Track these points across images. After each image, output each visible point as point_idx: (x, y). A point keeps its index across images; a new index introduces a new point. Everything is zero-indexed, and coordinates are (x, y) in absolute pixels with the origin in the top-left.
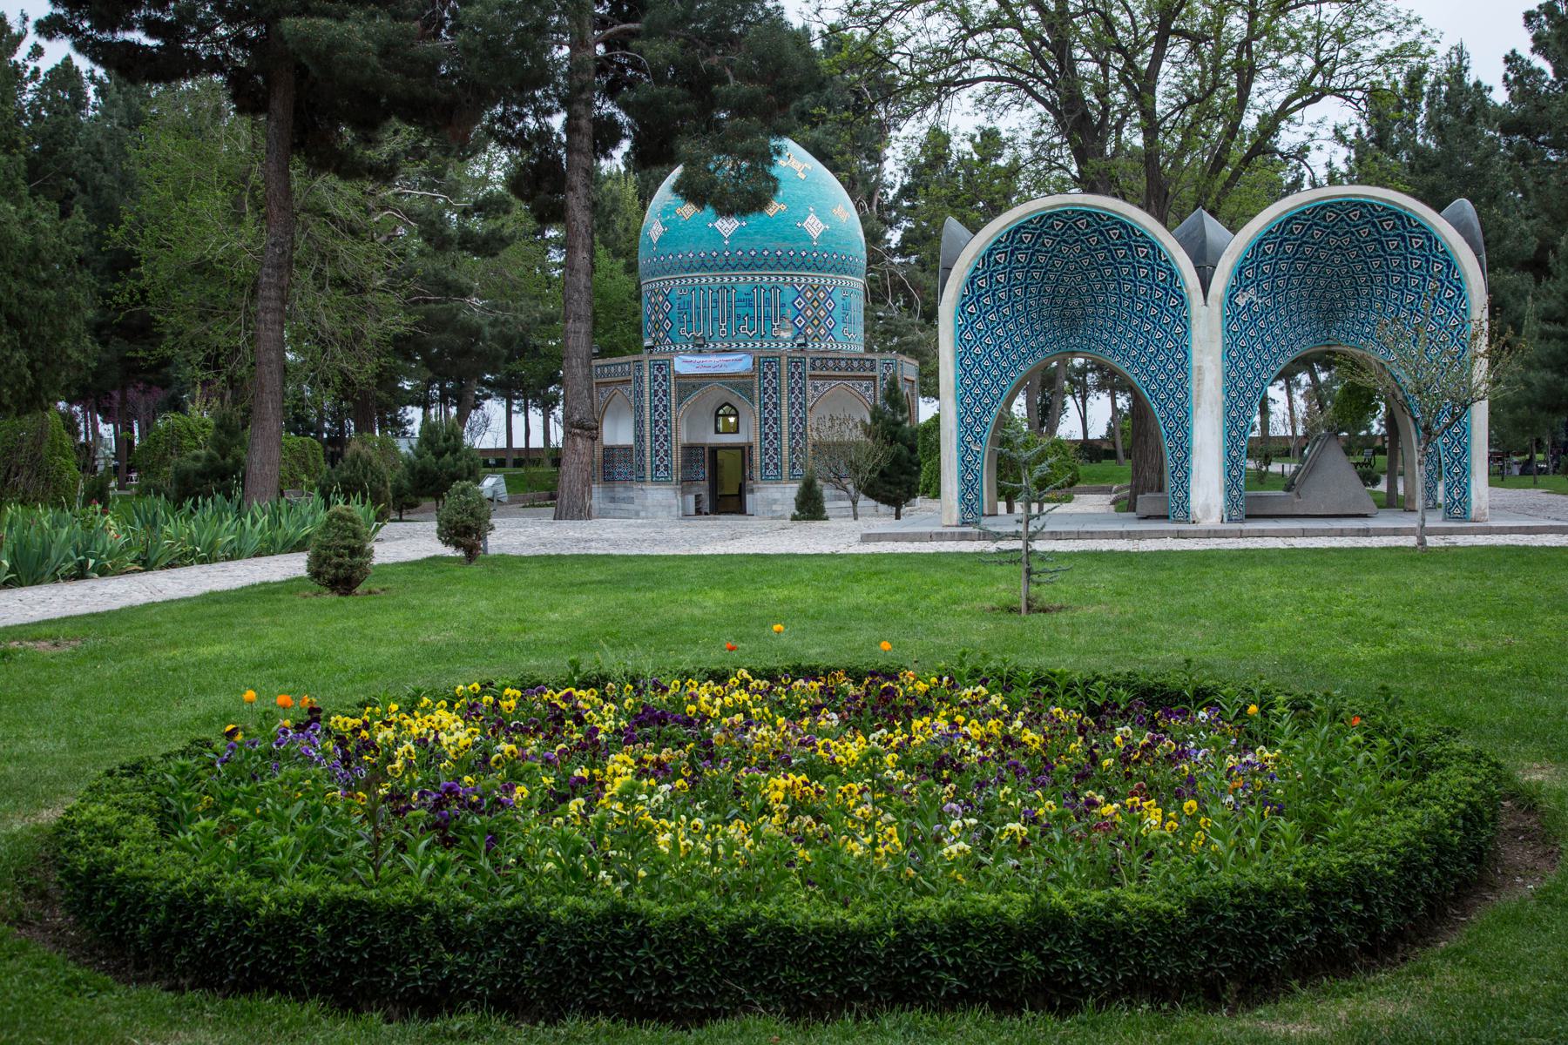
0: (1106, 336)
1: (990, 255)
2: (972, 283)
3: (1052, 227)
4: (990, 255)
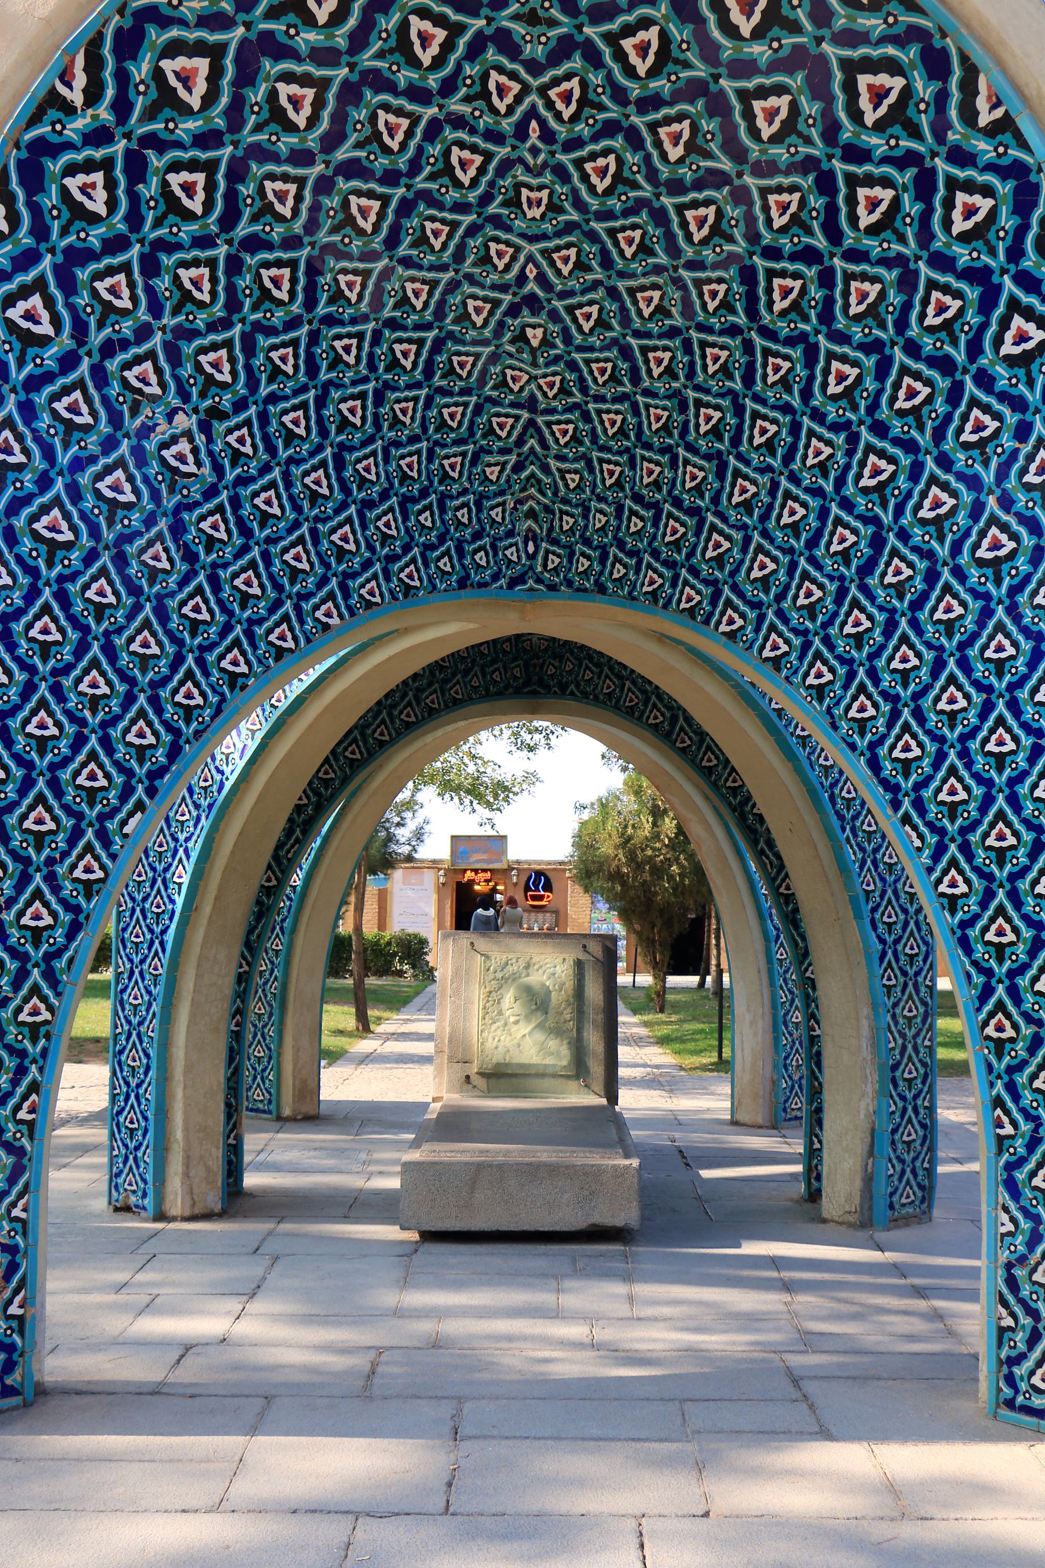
0: (675, 528)
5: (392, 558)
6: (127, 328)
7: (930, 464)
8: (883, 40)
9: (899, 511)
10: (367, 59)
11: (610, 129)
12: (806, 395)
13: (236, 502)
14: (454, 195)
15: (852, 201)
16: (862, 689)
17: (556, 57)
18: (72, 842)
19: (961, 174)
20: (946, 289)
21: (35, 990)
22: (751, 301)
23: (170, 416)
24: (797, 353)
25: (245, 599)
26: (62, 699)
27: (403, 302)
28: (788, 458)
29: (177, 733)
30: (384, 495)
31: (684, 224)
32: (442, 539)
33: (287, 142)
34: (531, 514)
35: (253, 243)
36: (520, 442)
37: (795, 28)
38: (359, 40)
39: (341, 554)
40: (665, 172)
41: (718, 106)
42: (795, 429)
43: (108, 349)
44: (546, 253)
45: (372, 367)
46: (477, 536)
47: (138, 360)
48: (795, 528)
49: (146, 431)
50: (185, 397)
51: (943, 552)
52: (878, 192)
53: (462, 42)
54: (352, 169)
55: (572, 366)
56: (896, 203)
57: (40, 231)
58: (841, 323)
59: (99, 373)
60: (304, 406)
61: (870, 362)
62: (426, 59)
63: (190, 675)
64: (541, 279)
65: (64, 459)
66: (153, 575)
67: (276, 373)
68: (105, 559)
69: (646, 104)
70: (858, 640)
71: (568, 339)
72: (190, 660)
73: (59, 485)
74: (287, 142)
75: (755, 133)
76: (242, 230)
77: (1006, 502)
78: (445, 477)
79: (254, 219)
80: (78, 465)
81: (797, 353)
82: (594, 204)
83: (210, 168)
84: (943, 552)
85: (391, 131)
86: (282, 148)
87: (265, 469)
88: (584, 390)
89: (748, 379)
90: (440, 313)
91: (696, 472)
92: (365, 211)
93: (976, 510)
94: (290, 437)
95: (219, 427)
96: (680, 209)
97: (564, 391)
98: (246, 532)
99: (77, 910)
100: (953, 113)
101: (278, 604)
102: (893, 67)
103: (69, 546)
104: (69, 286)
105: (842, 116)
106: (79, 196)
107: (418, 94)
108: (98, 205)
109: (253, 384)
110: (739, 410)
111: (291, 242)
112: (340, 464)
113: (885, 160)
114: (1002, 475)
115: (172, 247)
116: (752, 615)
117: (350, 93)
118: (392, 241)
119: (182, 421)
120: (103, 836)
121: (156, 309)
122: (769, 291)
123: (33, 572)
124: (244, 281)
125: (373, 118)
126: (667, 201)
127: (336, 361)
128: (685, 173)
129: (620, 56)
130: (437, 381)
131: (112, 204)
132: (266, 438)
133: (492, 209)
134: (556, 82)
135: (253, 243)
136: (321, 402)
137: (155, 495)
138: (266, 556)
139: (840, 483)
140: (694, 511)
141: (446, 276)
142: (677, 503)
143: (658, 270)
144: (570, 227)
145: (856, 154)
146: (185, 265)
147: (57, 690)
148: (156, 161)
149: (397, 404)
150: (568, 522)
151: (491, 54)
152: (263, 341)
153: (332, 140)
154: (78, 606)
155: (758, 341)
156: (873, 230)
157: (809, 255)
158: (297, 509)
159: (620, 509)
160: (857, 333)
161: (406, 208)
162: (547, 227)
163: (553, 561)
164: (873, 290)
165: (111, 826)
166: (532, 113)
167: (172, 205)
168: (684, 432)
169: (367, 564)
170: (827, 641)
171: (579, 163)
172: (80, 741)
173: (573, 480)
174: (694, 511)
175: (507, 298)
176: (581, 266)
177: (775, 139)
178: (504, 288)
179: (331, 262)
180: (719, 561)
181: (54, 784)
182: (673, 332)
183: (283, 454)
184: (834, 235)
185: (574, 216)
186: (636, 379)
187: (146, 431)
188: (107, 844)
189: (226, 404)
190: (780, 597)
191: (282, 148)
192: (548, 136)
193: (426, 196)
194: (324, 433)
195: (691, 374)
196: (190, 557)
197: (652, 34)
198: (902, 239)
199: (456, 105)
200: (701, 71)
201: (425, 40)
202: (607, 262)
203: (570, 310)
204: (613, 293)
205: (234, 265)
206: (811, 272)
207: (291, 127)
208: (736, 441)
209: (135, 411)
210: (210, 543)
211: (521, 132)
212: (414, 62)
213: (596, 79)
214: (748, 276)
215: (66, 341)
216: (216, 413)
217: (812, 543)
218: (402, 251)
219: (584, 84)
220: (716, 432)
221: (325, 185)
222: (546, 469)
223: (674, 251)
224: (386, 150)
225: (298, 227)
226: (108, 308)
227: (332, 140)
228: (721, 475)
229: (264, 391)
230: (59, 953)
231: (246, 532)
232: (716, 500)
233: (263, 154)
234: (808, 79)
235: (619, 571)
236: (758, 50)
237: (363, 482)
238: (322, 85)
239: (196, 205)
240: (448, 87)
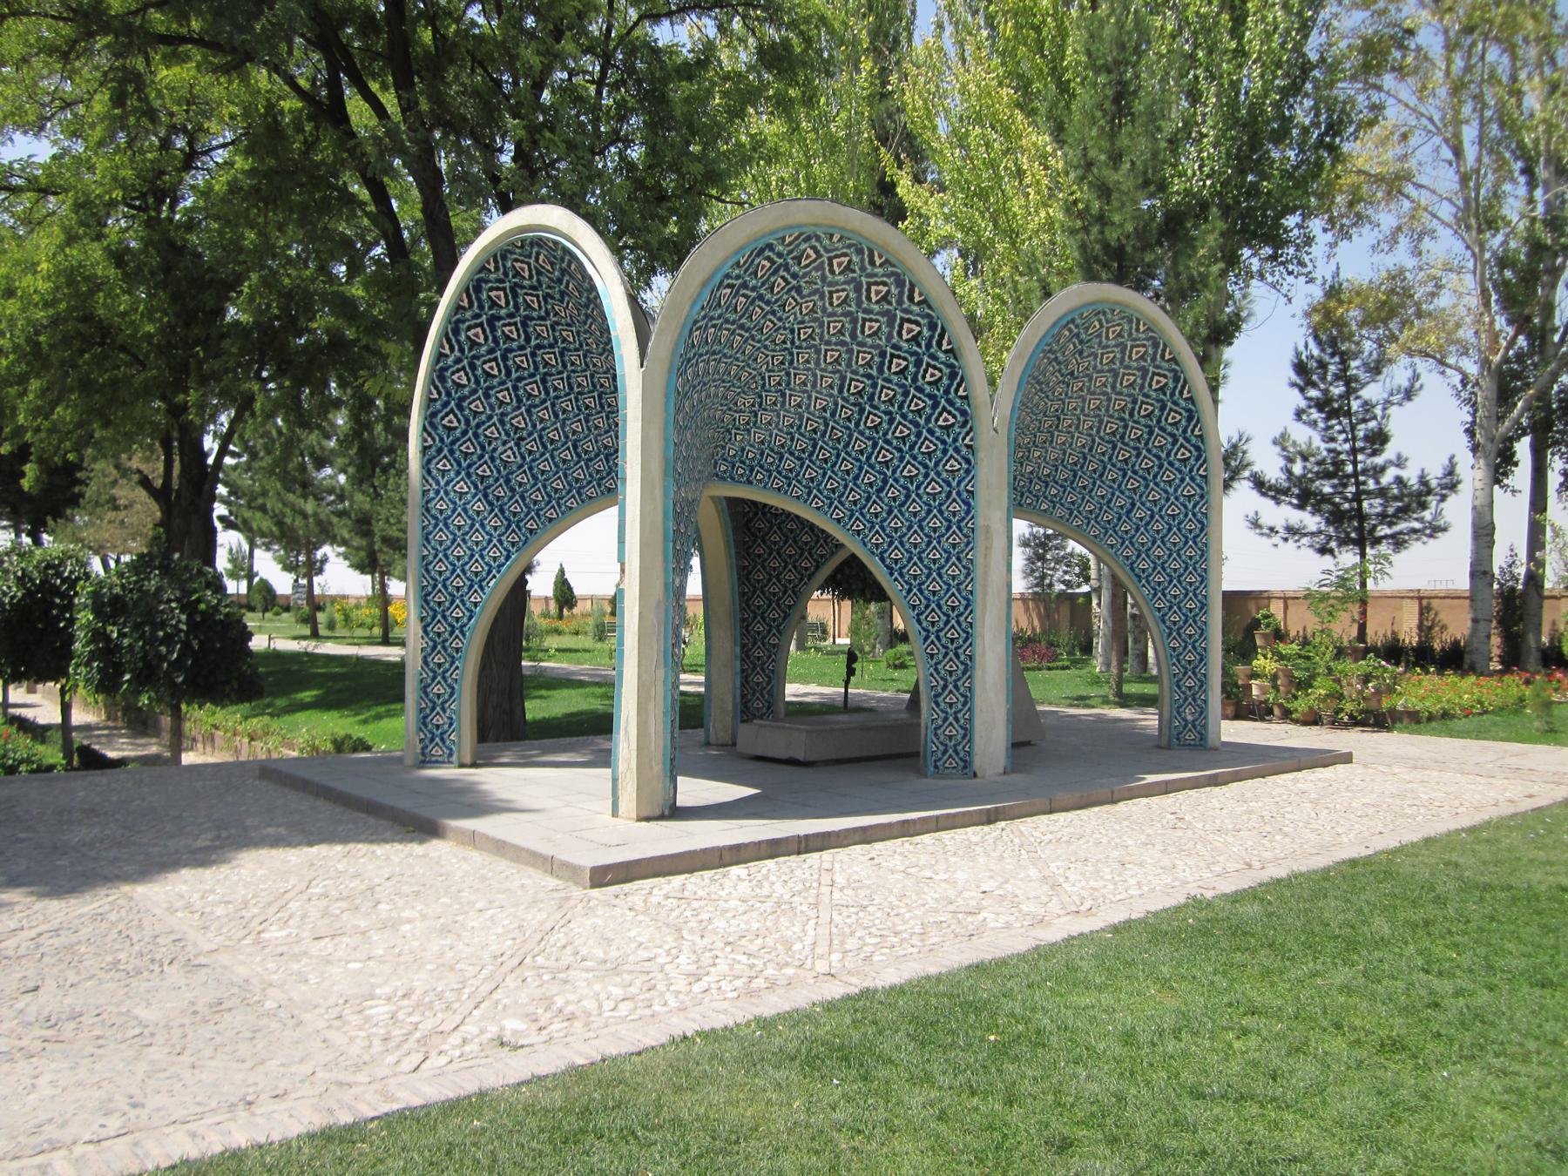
1: (456, 332)
2: (442, 379)
6: (483, 417)
13: (531, 469)
27: (579, 385)
30: (597, 455)
33: (515, 345)
35: (519, 379)
43: (478, 426)
49: (494, 450)
50: (508, 434)
54: (539, 347)
57: (448, 394)
65: (464, 465)
66: (498, 498)
67: (542, 420)
76: (514, 376)
80: (469, 466)
83: (495, 359)
104: (461, 409)
108: (465, 382)
109: (534, 426)
112: (575, 447)
115: (492, 388)
118: (564, 366)
121: (492, 409)
124: (521, 392)
127: (564, 411)
135: (519, 379)
136: (563, 426)
148: (478, 363)
153: (528, 339)
167: (488, 375)
187: (494, 450)
189: (525, 434)
196: (513, 490)
205: (515, 388)
210: (521, 484)
215: (463, 426)
237: (586, 452)
239: (496, 372)
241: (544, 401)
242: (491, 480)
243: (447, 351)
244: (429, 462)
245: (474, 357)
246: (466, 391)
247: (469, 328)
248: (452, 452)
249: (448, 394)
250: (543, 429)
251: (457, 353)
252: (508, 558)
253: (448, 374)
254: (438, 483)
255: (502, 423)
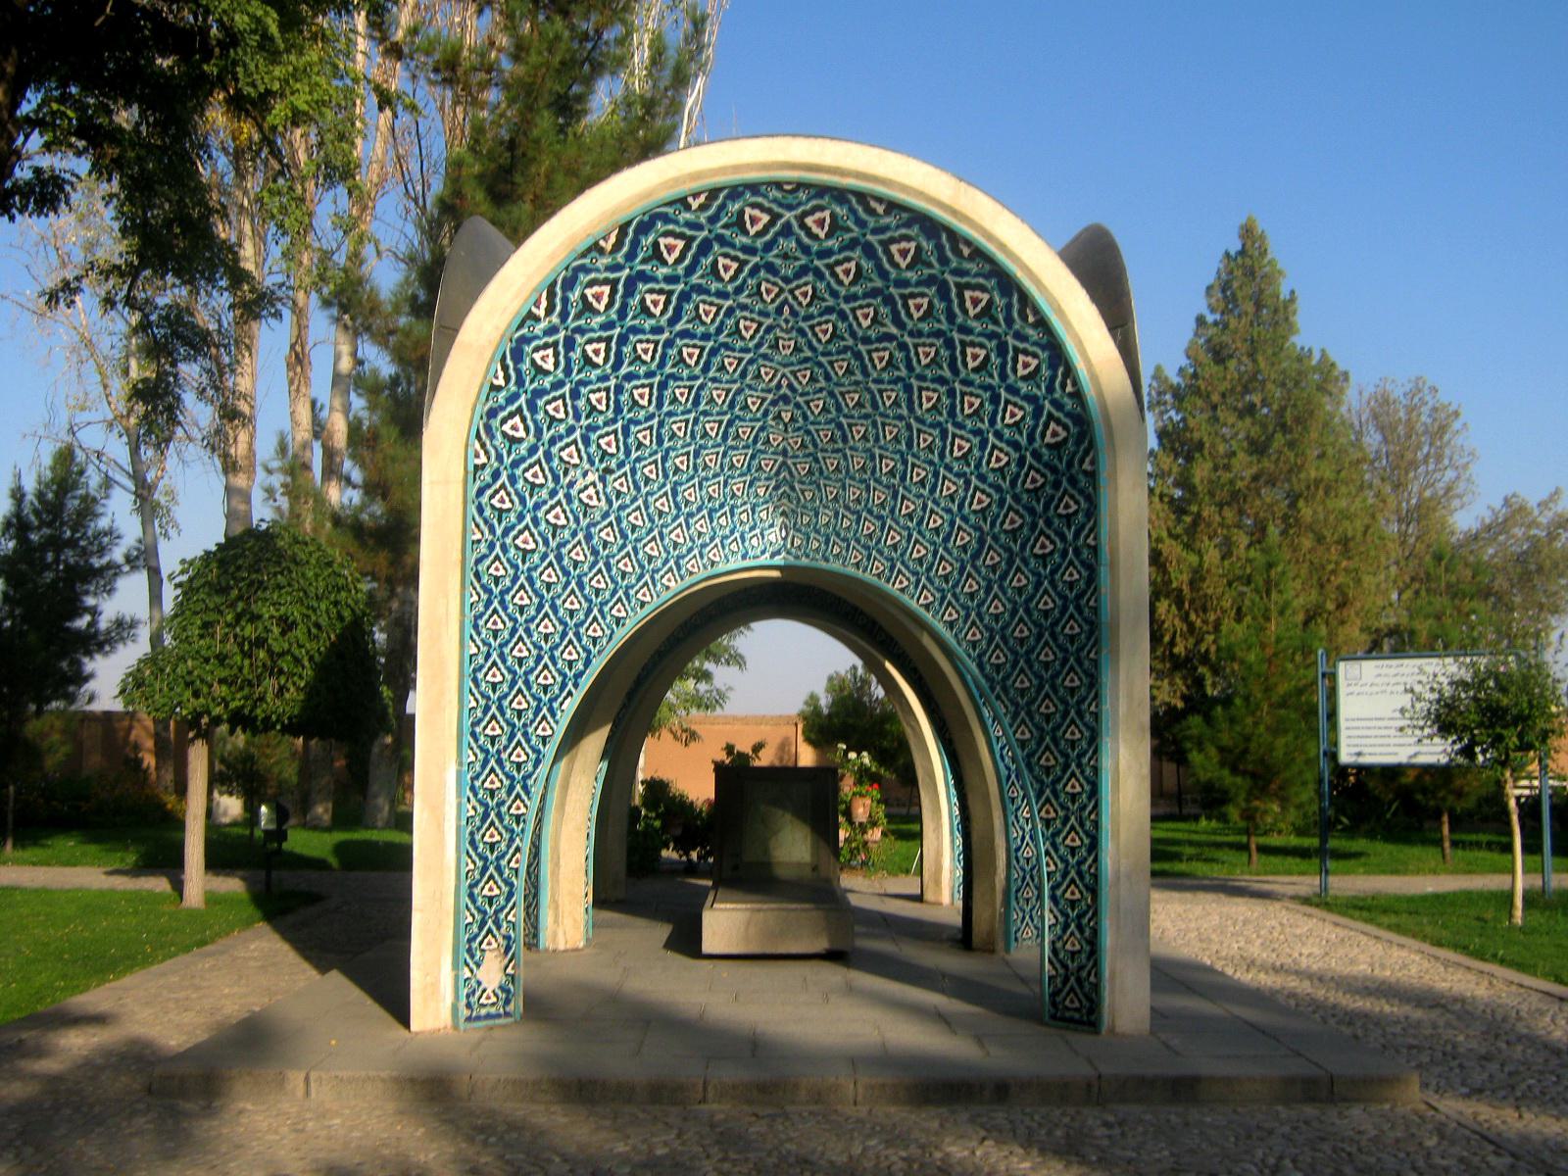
0: (869, 526)
1: (569, 284)
2: (518, 355)
3: (739, 223)
4: (569, 284)
5: (704, 546)
6: (562, 428)
7: (1009, 499)
8: (977, 275)
9: (993, 524)
10: (695, 279)
11: (829, 310)
12: (942, 456)
13: (619, 520)
14: (740, 344)
15: (964, 354)
16: (973, 623)
17: (798, 275)
18: (536, 714)
19: (1021, 346)
20: (1015, 405)
21: (518, 796)
22: (910, 402)
23: (585, 474)
24: (936, 432)
25: (624, 575)
26: (530, 636)
27: (711, 400)
28: (933, 490)
29: (589, 652)
30: (699, 509)
31: (871, 360)
32: (732, 532)
33: (649, 323)
34: (783, 514)
35: (629, 377)
36: (778, 473)
37: (930, 265)
38: (690, 270)
39: (676, 545)
40: (860, 333)
41: (889, 300)
42: (936, 474)
43: (553, 441)
44: (794, 373)
45: (693, 436)
46: (752, 529)
47: (568, 445)
48: (937, 530)
50: (591, 462)
51: (1016, 548)
52: (977, 350)
53: (746, 269)
54: (684, 334)
55: (808, 432)
56: (987, 358)
57: (520, 382)
58: (960, 418)
59: (548, 456)
60: (655, 462)
61: (976, 441)
62: (727, 277)
63: (595, 619)
64: (790, 386)
66: (576, 564)
67: (640, 445)
68: (552, 557)
69: (848, 299)
70: (972, 596)
71: (805, 418)
72: (595, 611)
73: (528, 519)
74: (649, 323)
75: (910, 316)
76: (623, 371)
77: (1049, 523)
78: (734, 495)
79: (631, 364)
80: (537, 507)
81: (936, 432)
82: (820, 348)
84: (1016, 548)
85: (707, 314)
86: (647, 326)
87: (634, 500)
88: (815, 445)
89: (909, 445)
90: (732, 406)
91: (879, 496)
92: (691, 354)
93: (1033, 526)
94: (647, 481)
95: (610, 478)
96: (869, 352)
97: (803, 446)
98: (624, 536)
99: (538, 752)
100: (1015, 315)
101: (641, 576)
102: (983, 289)
103: (533, 551)
105: (957, 310)
106: (539, 362)
107: (722, 295)
109: (628, 453)
110: (905, 462)
111: (650, 374)
112: (675, 493)
113: (980, 334)
114: (1047, 507)
116: (913, 579)
117: (685, 297)
118: (706, 369)
119: (592, 477)
120: (551, 711)
121: (577, 417)
122: (920, 397)
123: (515, 567)
125: (697, 308)
126: (862, 348)
128: (872, 334)
129: (834, 275)
130: (730, 442)
131: (556, 365)
132: (635, 482)
133: (764, 350)
134: (798, 287)
135: (629, 377)
136: (664, 459)
137: (577, 520)
138: (635, 549)
139: (961, 506)
140: (879, 517)
141: (735, 387)
142: (870, 512)
143: (857, 383)
144: (806, 360)
145: (965, 330)
146: (593, 392)
147: (527, 631)
148: (579, 339)
149: (709, 457)
150: (806, 519)
151: (762, 273)
152: (633, 429)
153: (673, 322)
154: (538, 584)
155: (915, 425)
156: (976, 370)
157: (942, 381)
158: (652, 520)
159: (836, 514)
160: (969, 424)
161: (713, 352)
162: (793, 359)
163: (797, 542)
164: (977, 402)
165: (556, 705)
166: (785, 302)
168: (873, 472)
169: (690, 550)
170: (954, 595)
171: (812, 327)
172: (539, 658)
173: (809, 495)
174: (879, 517)
175: (770, 397)
176: (813, 379)
177: (921, 319)
178: (769, 391)
179: (671, 383)
180: (895, 547)
181: (527, 683)
182: (866, 417)
183: (644, 491)
184: (955, 371)
185: (808, 354)
186: (845, 439)
187: (571, 484)
188: (553, 715)
189: (613, 466)
190: (929, 569)
191: (647, 326)
192: (794, 313)
193: (726, 346)
194: (666, 476)
195: (877, 440)
197: (852, 265)
198: (991, 376)
199: (743, 299)
200: (879, 283)
201: (726, 268)
202: (828, 378)
203: (807, 403)
204: (832, 394)
205: (619, 389)
206: (943, 389)
207: (651, 315)
208: (903, 479)
209: (566, 473)
210: (605, 544)
211: (779, 311)
212: (720, 279)
213: (821, 286)
214: (908, 389)
215: (532, 439)
216: (608, 471)
217: (946, 539)
218: (711, 374)
219: (814, 289)
220: (892, 473)
221: (669, 344)
222: (793, 488)
223: (865, 373)
224: (703, 323)
225: (653, 366)
226: (553, 419)
227: (673, 322)
228: (895, 496)
229: (634, 456)
230: (530, 776)
231: (624, 536)
232: (892, 511)
233: (635, 330)
234: (938, 291)
235: (836, 550)
236: (911, 276)
237: (687, 503)
238: (670, 293)
239: (599, 360)
240: (739, 290)
241: (651, 417)
242: (567, 534)
243: (541, 313)
244: (480, 492)
245: (580, 330)
246: (547, 382)
247: (591, 284)
248: (513, 479)
249: (520, 382)
250: (638, 460)
251: (555, 319)
252: (587, 663)
253: (528, 349)
254: (492, 530)
255: (586, 441)
